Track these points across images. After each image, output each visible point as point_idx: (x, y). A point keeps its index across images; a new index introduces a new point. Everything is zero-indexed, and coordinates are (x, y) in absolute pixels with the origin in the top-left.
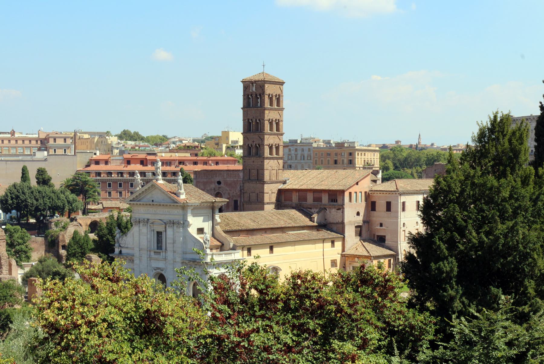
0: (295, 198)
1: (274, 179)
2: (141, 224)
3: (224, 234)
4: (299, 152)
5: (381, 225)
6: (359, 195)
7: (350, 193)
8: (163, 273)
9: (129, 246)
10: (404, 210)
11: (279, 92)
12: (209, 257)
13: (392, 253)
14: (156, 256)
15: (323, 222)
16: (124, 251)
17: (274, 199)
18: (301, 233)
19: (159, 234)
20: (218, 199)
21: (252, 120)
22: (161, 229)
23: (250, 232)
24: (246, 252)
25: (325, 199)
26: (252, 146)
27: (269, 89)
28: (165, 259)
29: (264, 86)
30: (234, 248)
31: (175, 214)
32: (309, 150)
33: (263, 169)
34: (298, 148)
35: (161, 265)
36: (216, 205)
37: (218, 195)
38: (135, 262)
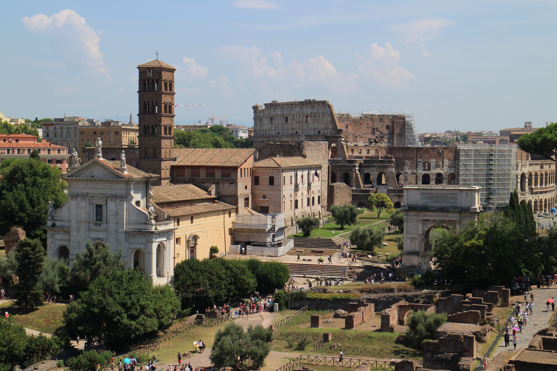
1: (168, 157)
2: (79, 199)
4: (65, 131)
5: (264, 197)
7: (241, 169)
9: (63, 219)
11: (171, 78)
14: (96, 228)
16: (57, 223)
17: (168, 175)
20: (153, 175)
21: (148, 103)
22: (99, 202)
24: (176, 223)
25: (218, 174)
27: (165, 76)
28: (106, 230)
30: (169, 218)
32: (75, 128)
33: (160, 148)
35: (101, 235)
38: (72, 233)
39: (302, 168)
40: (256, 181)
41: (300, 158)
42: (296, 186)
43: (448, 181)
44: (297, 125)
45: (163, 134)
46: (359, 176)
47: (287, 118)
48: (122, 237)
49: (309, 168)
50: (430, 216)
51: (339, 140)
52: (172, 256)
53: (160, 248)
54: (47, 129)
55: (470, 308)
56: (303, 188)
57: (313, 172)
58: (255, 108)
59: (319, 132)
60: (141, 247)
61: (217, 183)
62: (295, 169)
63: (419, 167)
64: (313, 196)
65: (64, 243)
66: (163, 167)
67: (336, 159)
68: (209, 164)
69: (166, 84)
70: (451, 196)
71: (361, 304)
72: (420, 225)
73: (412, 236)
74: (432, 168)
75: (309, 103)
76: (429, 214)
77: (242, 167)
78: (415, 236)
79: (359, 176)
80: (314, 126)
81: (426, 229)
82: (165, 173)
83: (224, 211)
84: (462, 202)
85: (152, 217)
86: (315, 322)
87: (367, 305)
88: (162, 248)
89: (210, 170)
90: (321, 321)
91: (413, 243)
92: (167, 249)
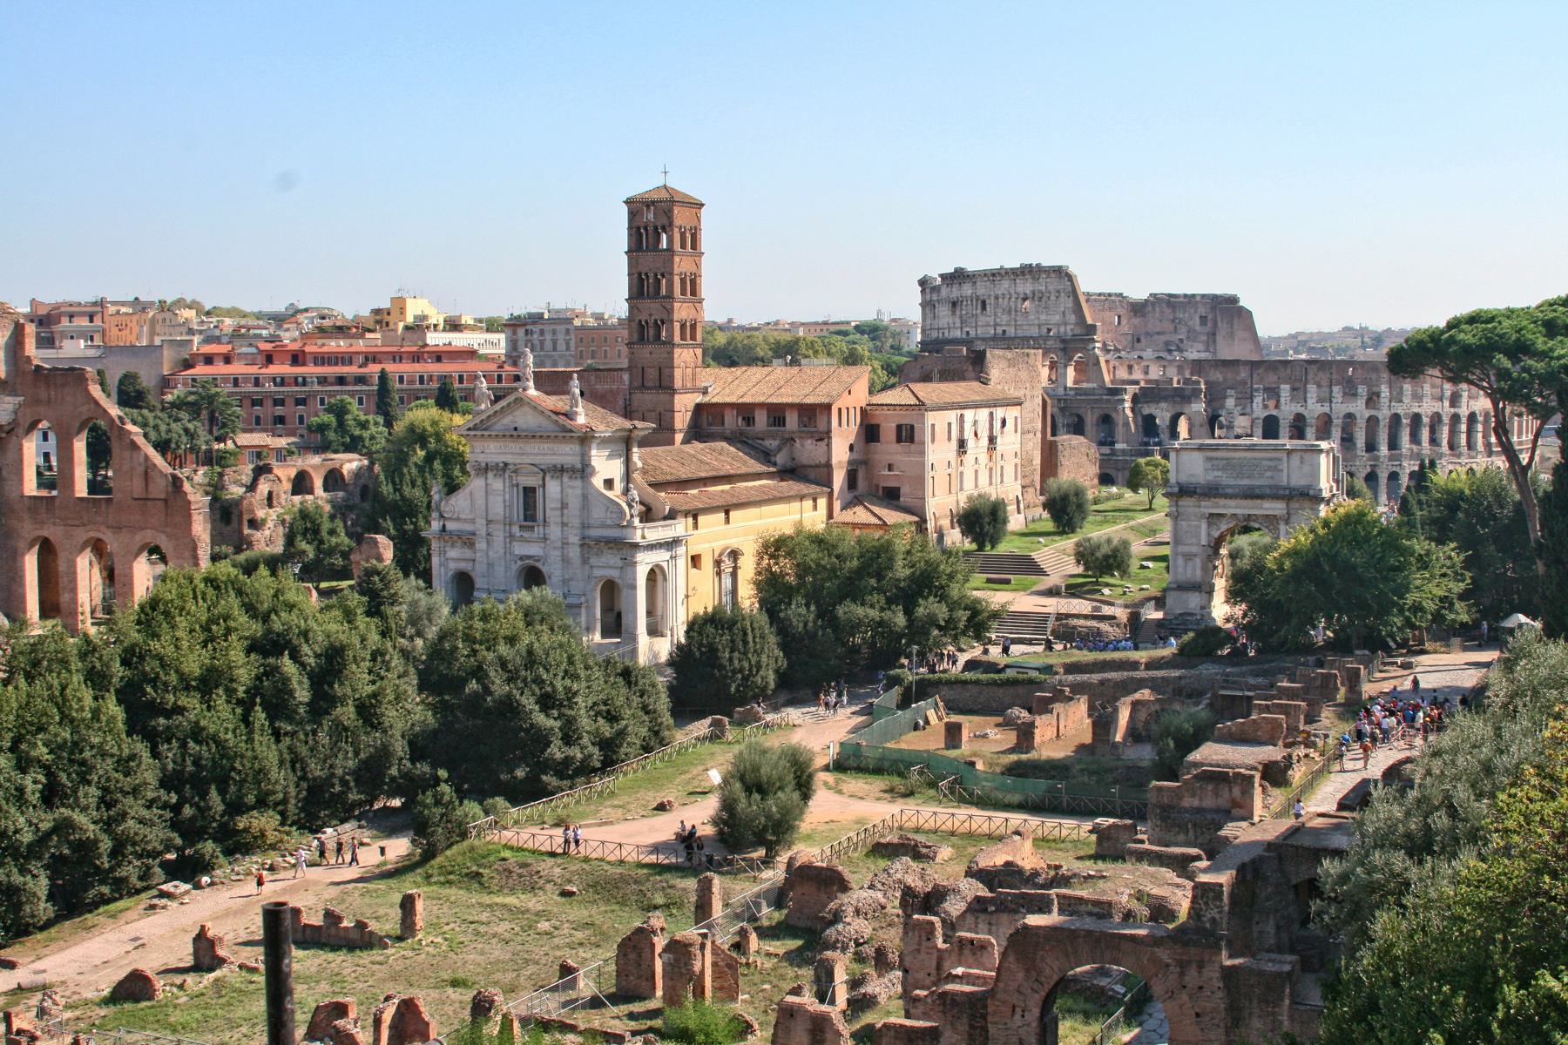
0: (731, 421)
2: (490, 475)
5: (890, 468)
8: (539, 565)
10: (933, 441)
12: (639, 532)
14: (526, 535)
15: (789, 465)
16: (450, 526)
19: (529, 492)
23: (682, 484)
27: (680, 217)
28: (545, 539)
29: (671, 211)
30: (672, 515)
31: (566, 453)
32: (568, 331)
34: (546, 328)
35: (534, 550)
40: (870, 432)
41: (975, 384)
42: (962, 444)
43: (1318, 430)
44: (1005, 318)
45: (677, 339)
47: (984, 303)
48: (574, 553)
50: (1225, 506)
52: (681, 596)
53: (654, 575)
54: (515, 333)
55: (1267, 709)
56: (978, 448)
57: (999, 413)
58: (923, 283)
60: (614, 574)
65: (463, 566)
66: (677, 407)
67: (1085, 385)
69: (683, 235)
71: (1059, 696)
72: (1204, 526)
73: (1186, 549)
74: (1282, 400)
75: (1028, 271)
76: (1222, 502)
78: (1194, 549)
80: (1033, 318)
81: (1216, 534)
82: (682, 420)
84: (1293, 476)
85: (635, 512)
86: (953, 733)
87: (1071, 699)
88: (659, 578)
89: (777, 413)
90: (965, 734)
91: (1190, 564)
92: (669, 577)
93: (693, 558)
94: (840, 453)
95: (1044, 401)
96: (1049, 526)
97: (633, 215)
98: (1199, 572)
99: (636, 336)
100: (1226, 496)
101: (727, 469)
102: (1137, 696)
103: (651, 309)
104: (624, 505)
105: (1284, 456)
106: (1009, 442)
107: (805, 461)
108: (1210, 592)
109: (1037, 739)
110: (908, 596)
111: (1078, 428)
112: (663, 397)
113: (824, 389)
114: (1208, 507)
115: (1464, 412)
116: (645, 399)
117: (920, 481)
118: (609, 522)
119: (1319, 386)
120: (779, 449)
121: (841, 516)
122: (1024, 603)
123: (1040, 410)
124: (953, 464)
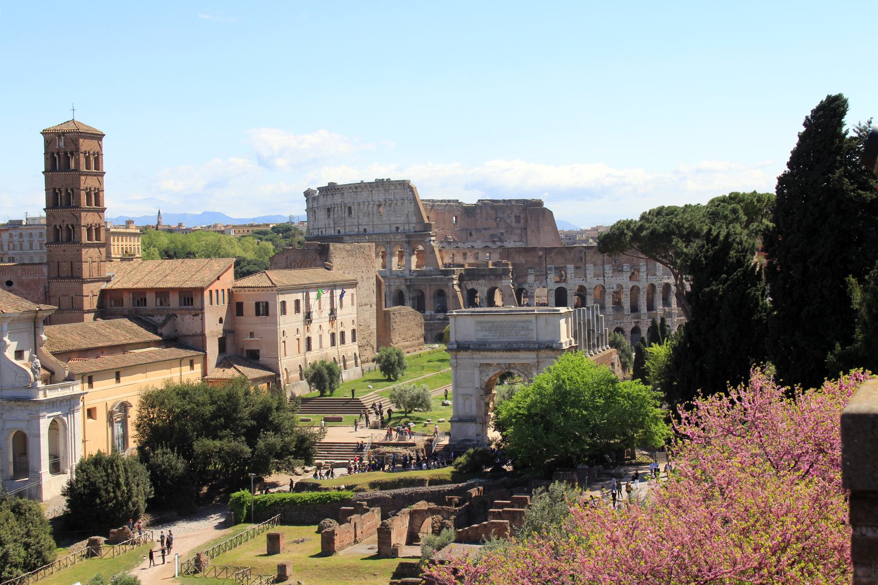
0: (128, 301)
1: (95, 275)
3: (53, 358)
4: (26, 239)
6: (220, 293)
7: (211, 291)
11: (97, 149)
12: (41, 393)
13: (272, 373)
18: (150, 352)
20: (43, 307)
21: (59, 190)
23: (84, 353)
24: (86, 385)
26: (61, 227)
27: (85, 145)
30: (71, 378)
33: (81, 261)
36: (40, 314)
37: (47, 301)
39: (318, 287)
40: (237, 308)
41: (321, 271)
44: (366, 219)
45: (85, 239)
46: (459, 294)
47: (350, 208)
49: (332, 287)
50: (491, 358)
51: (428, 239)
55: (499, 516)
57: (338, 292)
58: (307, 194)
59: (397, 228)
60: (22, 426)
61: (164, 317)
62: (305, 289)
63: (549, 277)
64: (342, 329)
67: (424, 268)
68: (161, 285)
69: (87, 159)
70: (523, 324)
72: (477, 372)
73: (464, 391)
74: (569, 276)
75: (381, 184)
76: (489, 354)
77: (213, 288)
78: (471, 391)
79: (459, 294)
81: (486, 379)
83: (180, 362)
86: (274, 545)
87: (368, 511)
88: (61, 428)
89: (163, 294)
90: (283, 543)
93: (89, 411)
94: (213, 325)
95: (378, 280)
96: (380, 375)
97: (48, 143)
98: (474, 408)
99: (52, 239)
100: (492, 350)
101: (122, 340)
102: (415, 507)
103: (64, 216)
104: (29, 371)
105: (533, 318)
106: (348, 314)
107: (185, 332)
108: (484, 424)
109: (337, 544)
110: (251, 436)
111: (400, 300)
112: (73, 284)
113: (199, 276)
114: (481, 358)
115: (643, 285)
116: (58, 287)
117: (274, 345)
118: (18, 385)
119: (595, 265)
120: (164, 323)
121: (215, 373)
122: (340, 434)
123: (374, 288)
124: (301, 330)
